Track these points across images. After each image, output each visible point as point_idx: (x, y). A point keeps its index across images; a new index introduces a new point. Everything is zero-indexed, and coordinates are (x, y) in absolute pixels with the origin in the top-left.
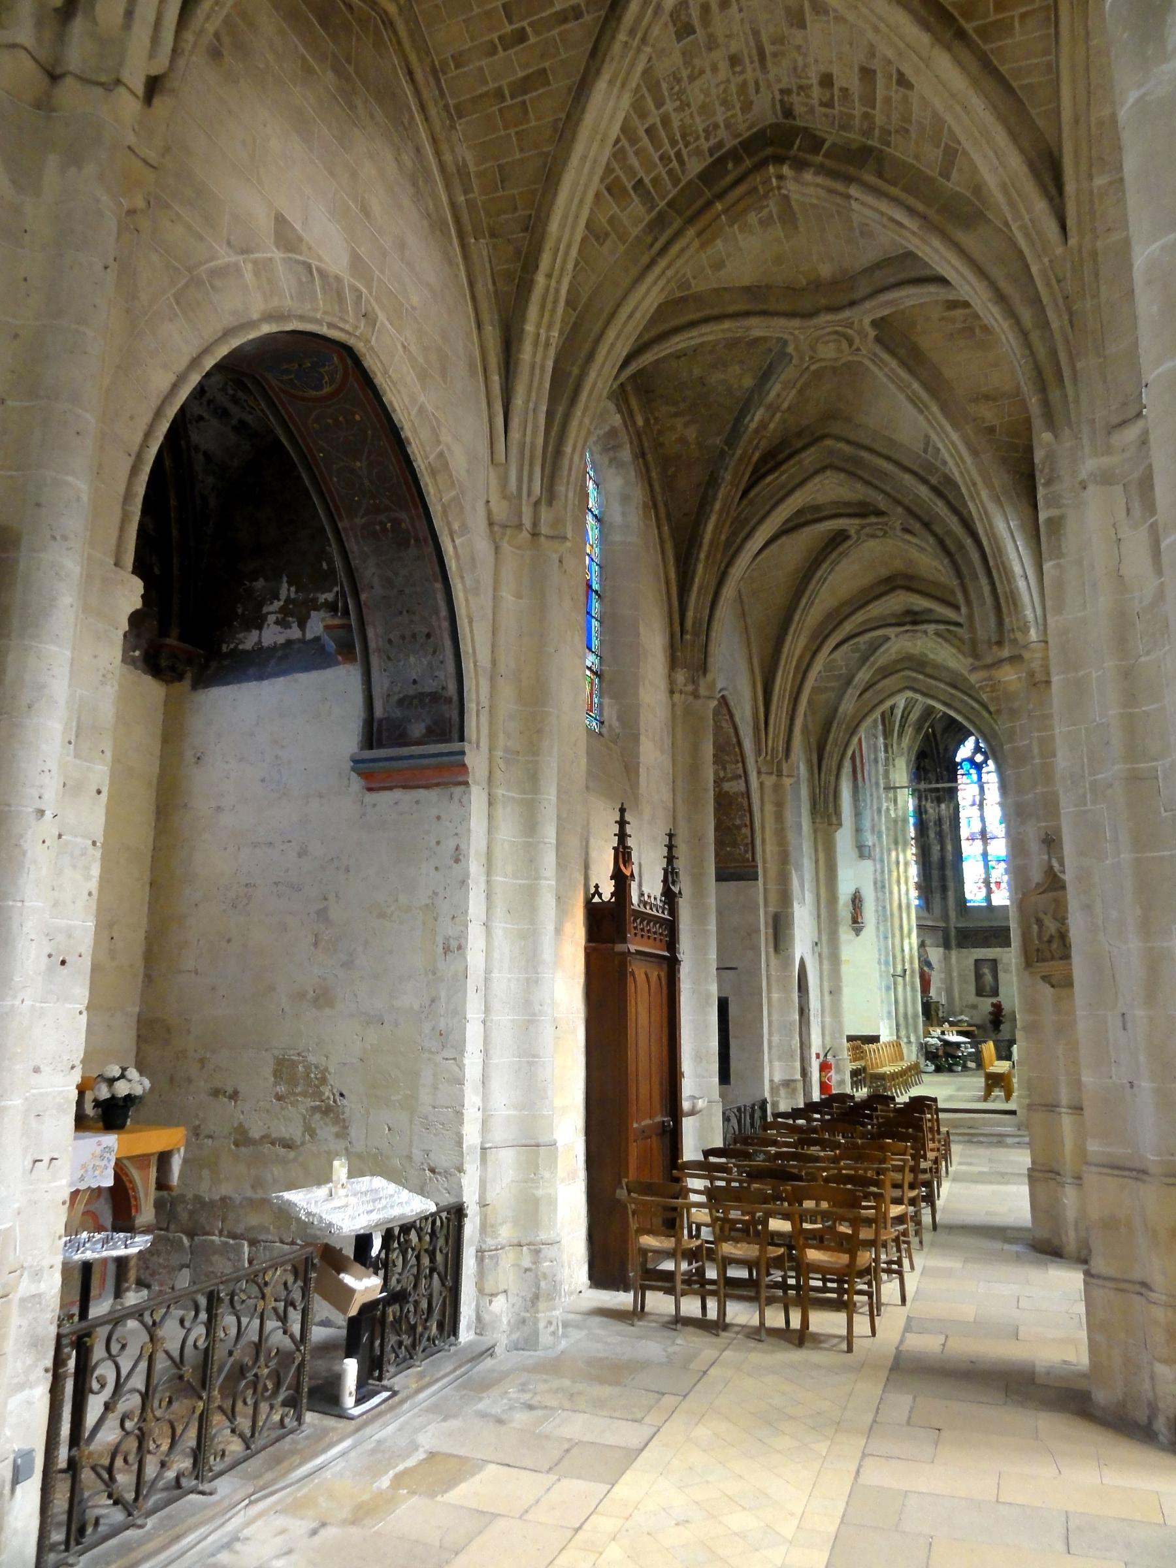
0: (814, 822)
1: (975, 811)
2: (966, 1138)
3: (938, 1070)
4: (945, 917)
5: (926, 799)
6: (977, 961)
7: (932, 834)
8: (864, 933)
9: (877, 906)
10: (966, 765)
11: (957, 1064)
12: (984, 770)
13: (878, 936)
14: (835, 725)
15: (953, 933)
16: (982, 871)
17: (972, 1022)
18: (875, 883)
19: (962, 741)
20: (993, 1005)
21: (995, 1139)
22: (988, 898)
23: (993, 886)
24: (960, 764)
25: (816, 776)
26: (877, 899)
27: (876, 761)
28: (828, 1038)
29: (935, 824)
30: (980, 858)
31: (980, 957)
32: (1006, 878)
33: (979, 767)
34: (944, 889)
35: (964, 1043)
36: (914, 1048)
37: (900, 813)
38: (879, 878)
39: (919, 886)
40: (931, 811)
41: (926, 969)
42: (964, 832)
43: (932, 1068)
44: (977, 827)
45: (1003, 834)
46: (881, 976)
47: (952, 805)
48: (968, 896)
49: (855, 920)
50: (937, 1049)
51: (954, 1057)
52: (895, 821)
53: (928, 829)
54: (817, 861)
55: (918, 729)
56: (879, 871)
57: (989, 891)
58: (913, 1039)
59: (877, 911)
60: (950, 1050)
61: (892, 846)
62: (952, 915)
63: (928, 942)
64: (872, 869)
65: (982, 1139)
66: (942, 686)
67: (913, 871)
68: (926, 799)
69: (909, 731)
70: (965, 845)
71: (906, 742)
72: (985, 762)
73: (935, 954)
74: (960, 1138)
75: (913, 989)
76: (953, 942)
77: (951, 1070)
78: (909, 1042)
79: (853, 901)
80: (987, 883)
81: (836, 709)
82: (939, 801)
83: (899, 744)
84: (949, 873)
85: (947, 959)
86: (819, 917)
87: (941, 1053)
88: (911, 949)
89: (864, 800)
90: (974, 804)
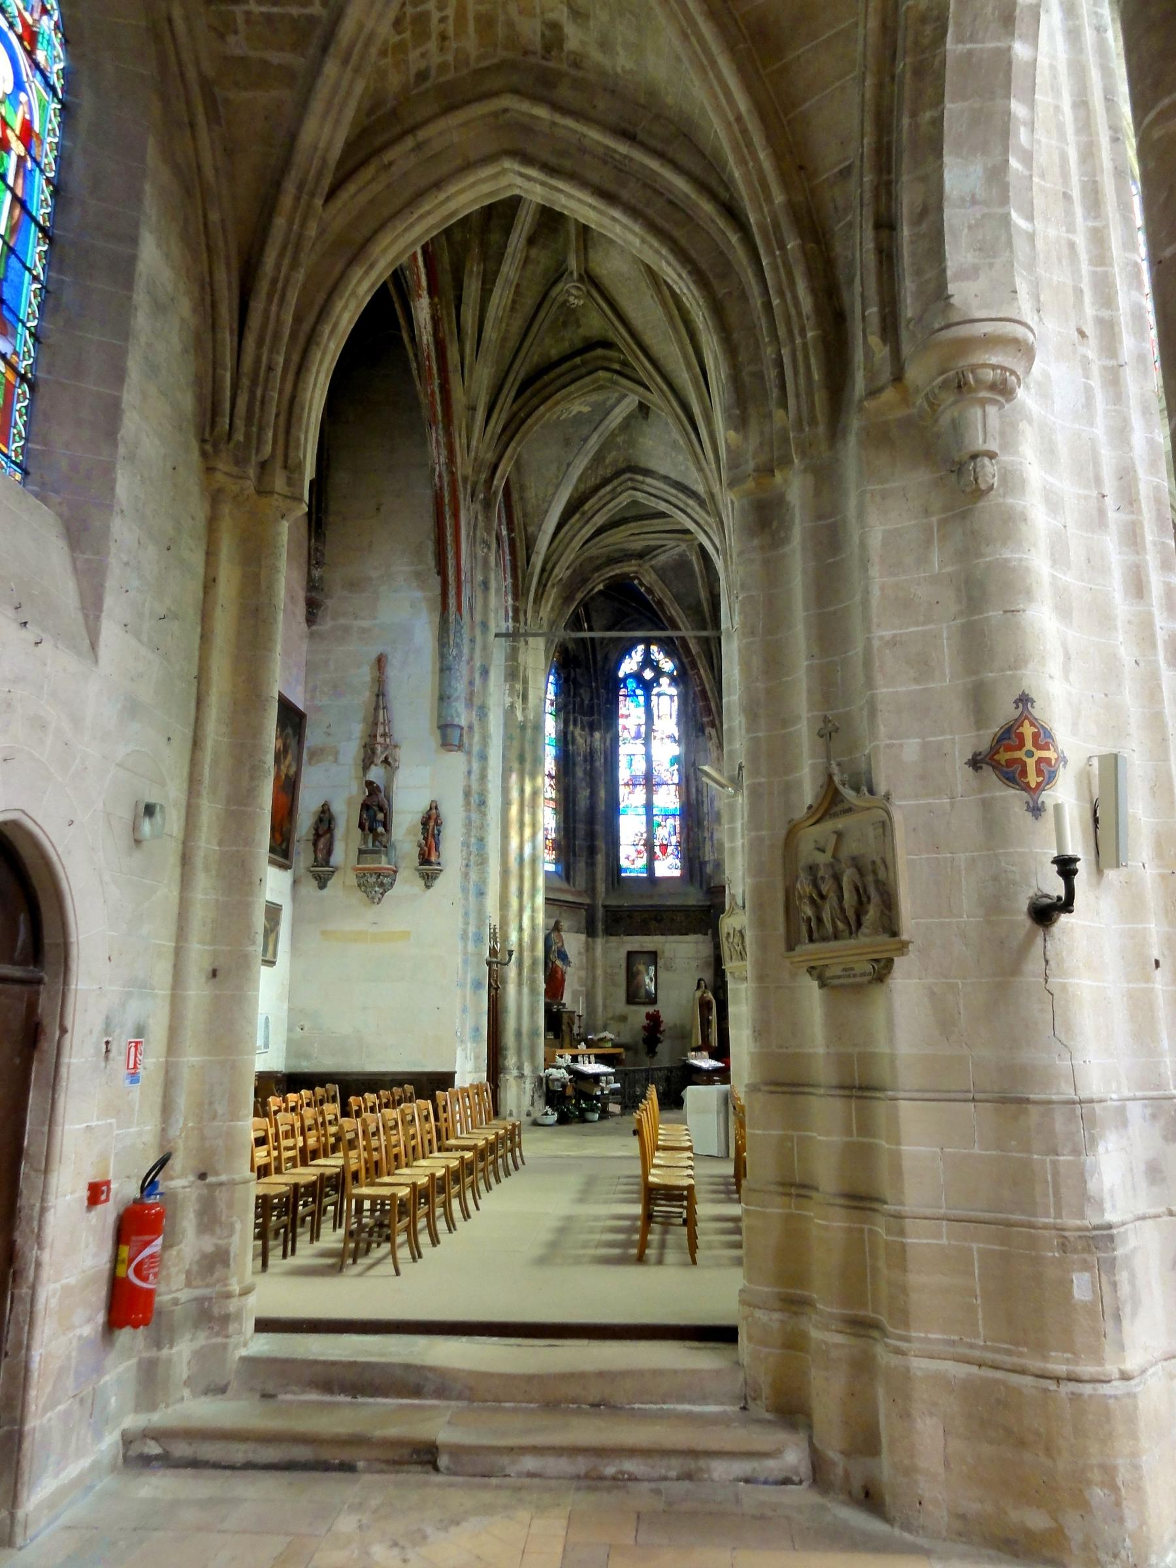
0: (210, 470)
1: (638, 748)
2: (581, 1465)
3: (563, 1120)
4: (591, 890)
5: (575, 724)
6: (630, 954)
7: (580, 773)
8: (439, 883)
9: (468, 834)
10: (631, 684)
11: (593, 1109)
12: (655, 691)
13: (465, 890)
14: (289, 188)
15: (600, 913)
16: (643, 828)
17: (617, 1040)
18: (467, 794)
19: (627, 651)
20: (648, 1016)
21: (674, 1466)
22: (650, 868)
23: (657, 849)
24: (624, 680)
25: (227, 339)
26: (468, 824)
27: (485, 585)
28: (182, 1122)
29: (585, 760)
30: (642, 811)
31: (636, 948)
32: (674, 840)
33: (647, 686)
34: (592, 851)
35: (606, 1075)
36: (528, 1086)
37: (531, 716)
38: (475, 786)
39: (557, 846)
40: (580, 741)
41: (559, 963)
42: (624, 775)
43: (555, 1117)
44: (640, 767)
45: (676, 779)
46: (465, 962)
47: (609, 736)
48: (624, 863)
49: (425, 860)
50: (564, 1086)
51: (589, 1097)
52: (523, 728)
53: (574, 764)
54: (209, 584)
55: (567, 599)
56: (475, 776)
57: (652, 858)
58: (527, 1070)
59: (466, 844)
60: (584, 1086)
61: (516, 765)
62: (601, 887)
63: (565, 924)
64: (463, 768)
65: (631, 1466)
66: (594, 135)
67: (548, 819)
68: (575, 724)
69: (552, 595)
70: (623, 791)
71: (546, 611)
72: (656, 680)
73: (573, 943)
74: (562, 1465)
75: (533, 991)
76: (600, 926)
77: (583, 1120)
78: (521, 1076)
79: (425, 823)
80: (649, 845)
81: (293, 137)
82: (592, 727)
83: (536, 611)
84: (599, 828)
85: (589, 949)
86: (196, 744)
87: (569, 1091)
88: (534, 927)
89: (457, 645)
90: (637, 736)
